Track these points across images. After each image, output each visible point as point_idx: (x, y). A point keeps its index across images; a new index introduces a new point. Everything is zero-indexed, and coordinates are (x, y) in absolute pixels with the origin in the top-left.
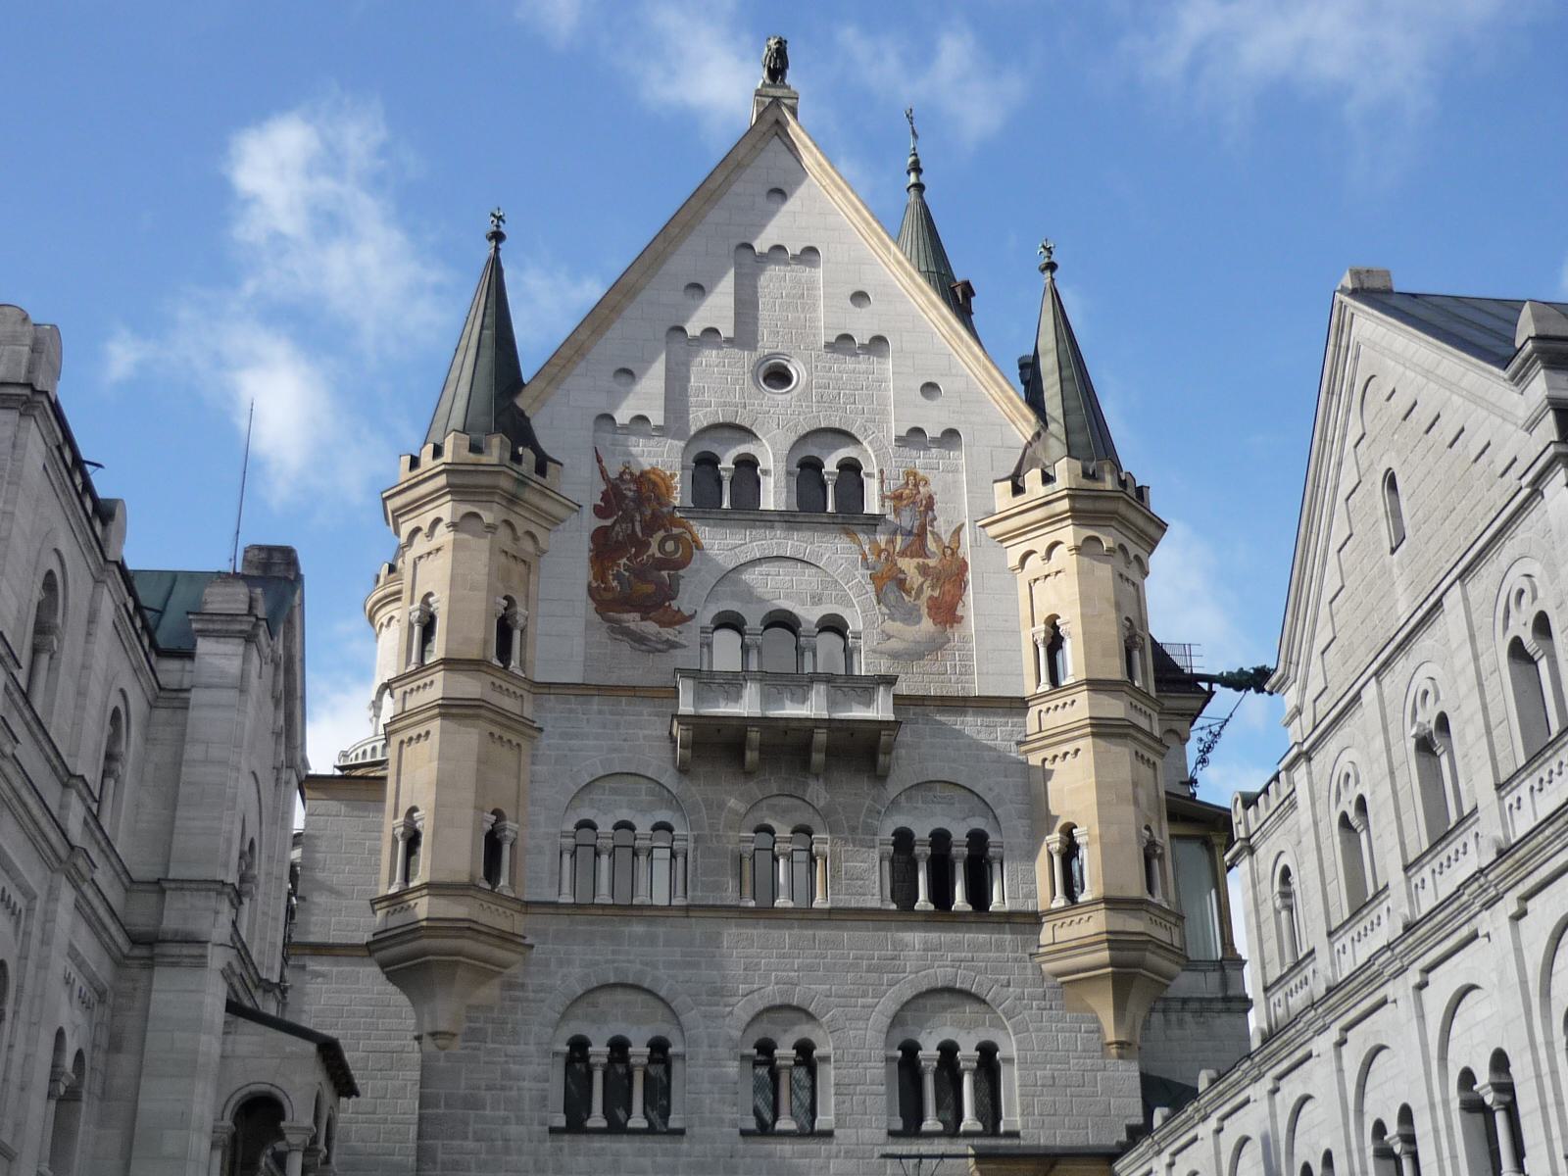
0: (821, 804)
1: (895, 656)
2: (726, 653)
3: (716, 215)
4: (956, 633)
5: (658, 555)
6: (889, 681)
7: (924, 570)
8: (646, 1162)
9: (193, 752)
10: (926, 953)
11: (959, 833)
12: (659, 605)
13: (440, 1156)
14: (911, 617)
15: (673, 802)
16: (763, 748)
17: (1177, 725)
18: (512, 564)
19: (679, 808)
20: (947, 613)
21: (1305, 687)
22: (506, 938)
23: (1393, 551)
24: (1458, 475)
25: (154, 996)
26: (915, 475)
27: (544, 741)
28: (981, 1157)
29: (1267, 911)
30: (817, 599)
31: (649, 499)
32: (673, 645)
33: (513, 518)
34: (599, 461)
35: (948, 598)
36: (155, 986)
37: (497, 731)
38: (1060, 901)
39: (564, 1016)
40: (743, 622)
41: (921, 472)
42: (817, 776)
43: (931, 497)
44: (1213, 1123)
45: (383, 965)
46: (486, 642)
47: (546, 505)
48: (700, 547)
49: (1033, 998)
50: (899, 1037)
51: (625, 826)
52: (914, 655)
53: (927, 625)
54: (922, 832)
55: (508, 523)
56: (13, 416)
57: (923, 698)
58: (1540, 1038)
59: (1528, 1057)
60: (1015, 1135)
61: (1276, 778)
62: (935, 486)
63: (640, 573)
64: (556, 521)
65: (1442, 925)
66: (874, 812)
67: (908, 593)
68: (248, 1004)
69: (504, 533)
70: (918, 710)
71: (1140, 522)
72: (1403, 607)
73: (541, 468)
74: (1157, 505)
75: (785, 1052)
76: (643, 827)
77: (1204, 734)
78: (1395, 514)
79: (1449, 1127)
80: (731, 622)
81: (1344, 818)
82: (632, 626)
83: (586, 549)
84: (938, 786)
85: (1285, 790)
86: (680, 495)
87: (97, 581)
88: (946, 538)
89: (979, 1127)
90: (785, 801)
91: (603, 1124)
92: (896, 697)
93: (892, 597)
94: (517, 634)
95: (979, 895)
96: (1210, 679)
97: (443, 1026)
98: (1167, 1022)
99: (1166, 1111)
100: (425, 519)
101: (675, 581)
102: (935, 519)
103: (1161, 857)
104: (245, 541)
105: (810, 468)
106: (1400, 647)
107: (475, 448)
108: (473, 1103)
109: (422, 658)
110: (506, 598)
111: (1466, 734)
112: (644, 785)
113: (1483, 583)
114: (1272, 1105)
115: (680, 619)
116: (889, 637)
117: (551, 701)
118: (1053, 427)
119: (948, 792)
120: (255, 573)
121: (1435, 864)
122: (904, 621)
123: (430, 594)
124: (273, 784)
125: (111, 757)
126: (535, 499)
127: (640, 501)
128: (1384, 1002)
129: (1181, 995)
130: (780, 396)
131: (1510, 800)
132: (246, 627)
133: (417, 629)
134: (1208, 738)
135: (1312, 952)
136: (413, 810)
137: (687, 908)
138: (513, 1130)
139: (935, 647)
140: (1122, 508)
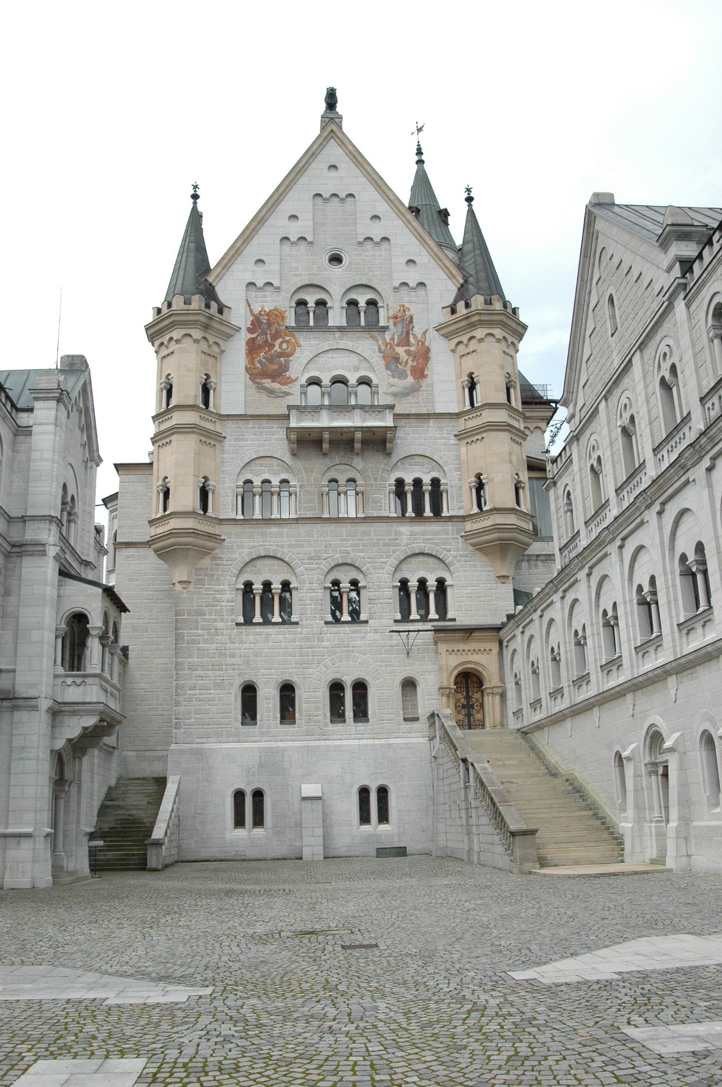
0: (359, 467)
1: (395, 395)
3: (303, 180)
4: (425, 382)
5: (279, 350)
6: (392, 407)
7: (408, 353)
8: (281, 637)
9: (36, 455)
11: (426, 480)
12: (280, 375)
13: (186, 638)
14: (402, 375)
16: (331, 442)
17: (540, 425)
18: (208, 358)
19: (292, 472)
20: (420, 373)
21: (576, 404)
23: (612, 335)
24: (639, 295)
25: (23, 570)
26: (403, 306)
27: (227, 443)
28: (437, 631)
29: (562, 511)
30: (356, 369)
31: (274, 323)
32: (287, 394)
33: (207, 336)
34: (249, 306)
35: (420, 366)
36: (23, 565)
37: (204, 439)
38: (476, 510)
39: (240, 571)
40: (321, 382)
41: (407, 305)
42: (358, 454)
43: (411, 317)
44: (539, 613)
45: (156, 551)
46: (196, 396)
47: (223, 328)
49: (462, 556)
50: (399, 576)
51: (266, 481)
52: (404, 394)
53: (410, 379)
54: (409, 479)
55: (204, 338)
57: (408, 415)
58: (668, 570)
59: (663, 579)
60: (454, 620)
61: (564, 449)
63: (271, 360)
65: (629, 517)
66: (385, 470)
67: (401, 364)
68: (73, 573)
70: (406, 421)
71: (514, 325)
72: (616, 362)
73: (220, 311)
74: (523, 317)
75: (345, 585)
76: (275, 482)
77: (553, 428)
78: (613, 316)
79: (632, 612)
80: (315, 382)
81: (592, 466)
82: (267, 385)
83: (244, 349)
84: (416, 457)
85: (568, 455)
86: (291, 321)
88: (419, 337)
89: (437, 617)
90: (343, 467)
91: (261, 620)
92: (395, 415)
93: (393, 366)
94: (211, 392)
95: (437, 509)
96: (556, 402)
97: (185, 578)
98: (530, 565)
99: (520, 607)
100: (165, 339)
101: (287, 362)
102: (413, 327)
103: (523, 488)
104: (62, 353)
105: (353, 303)
106: (614, 382)
107: (187, 302)
108: (200, 613)
109: (168, 404)
110: (206, 375)
111: (642, 426)
112: (275, 462)
113: (650, 351)
114: (562, 603)
115: (290, 381)
116: (392, 386)
118: (471, 279)
119: (421, 460)
120: (67, 368)
121: (628, 488)
122: (399, 378)
123: (169, 375)
124: (83, 469)
127: (269, 324)
128: (606, 555)
129: (536, 553)
130: (337, 270)
131: (659, 456)
132: (57, 395)
133: (165, 392)
134: (555, 430)
135: (578, 532)
136: (166, 478)
137: (297, 519)
138: (220, 625)
139: (414, 390)
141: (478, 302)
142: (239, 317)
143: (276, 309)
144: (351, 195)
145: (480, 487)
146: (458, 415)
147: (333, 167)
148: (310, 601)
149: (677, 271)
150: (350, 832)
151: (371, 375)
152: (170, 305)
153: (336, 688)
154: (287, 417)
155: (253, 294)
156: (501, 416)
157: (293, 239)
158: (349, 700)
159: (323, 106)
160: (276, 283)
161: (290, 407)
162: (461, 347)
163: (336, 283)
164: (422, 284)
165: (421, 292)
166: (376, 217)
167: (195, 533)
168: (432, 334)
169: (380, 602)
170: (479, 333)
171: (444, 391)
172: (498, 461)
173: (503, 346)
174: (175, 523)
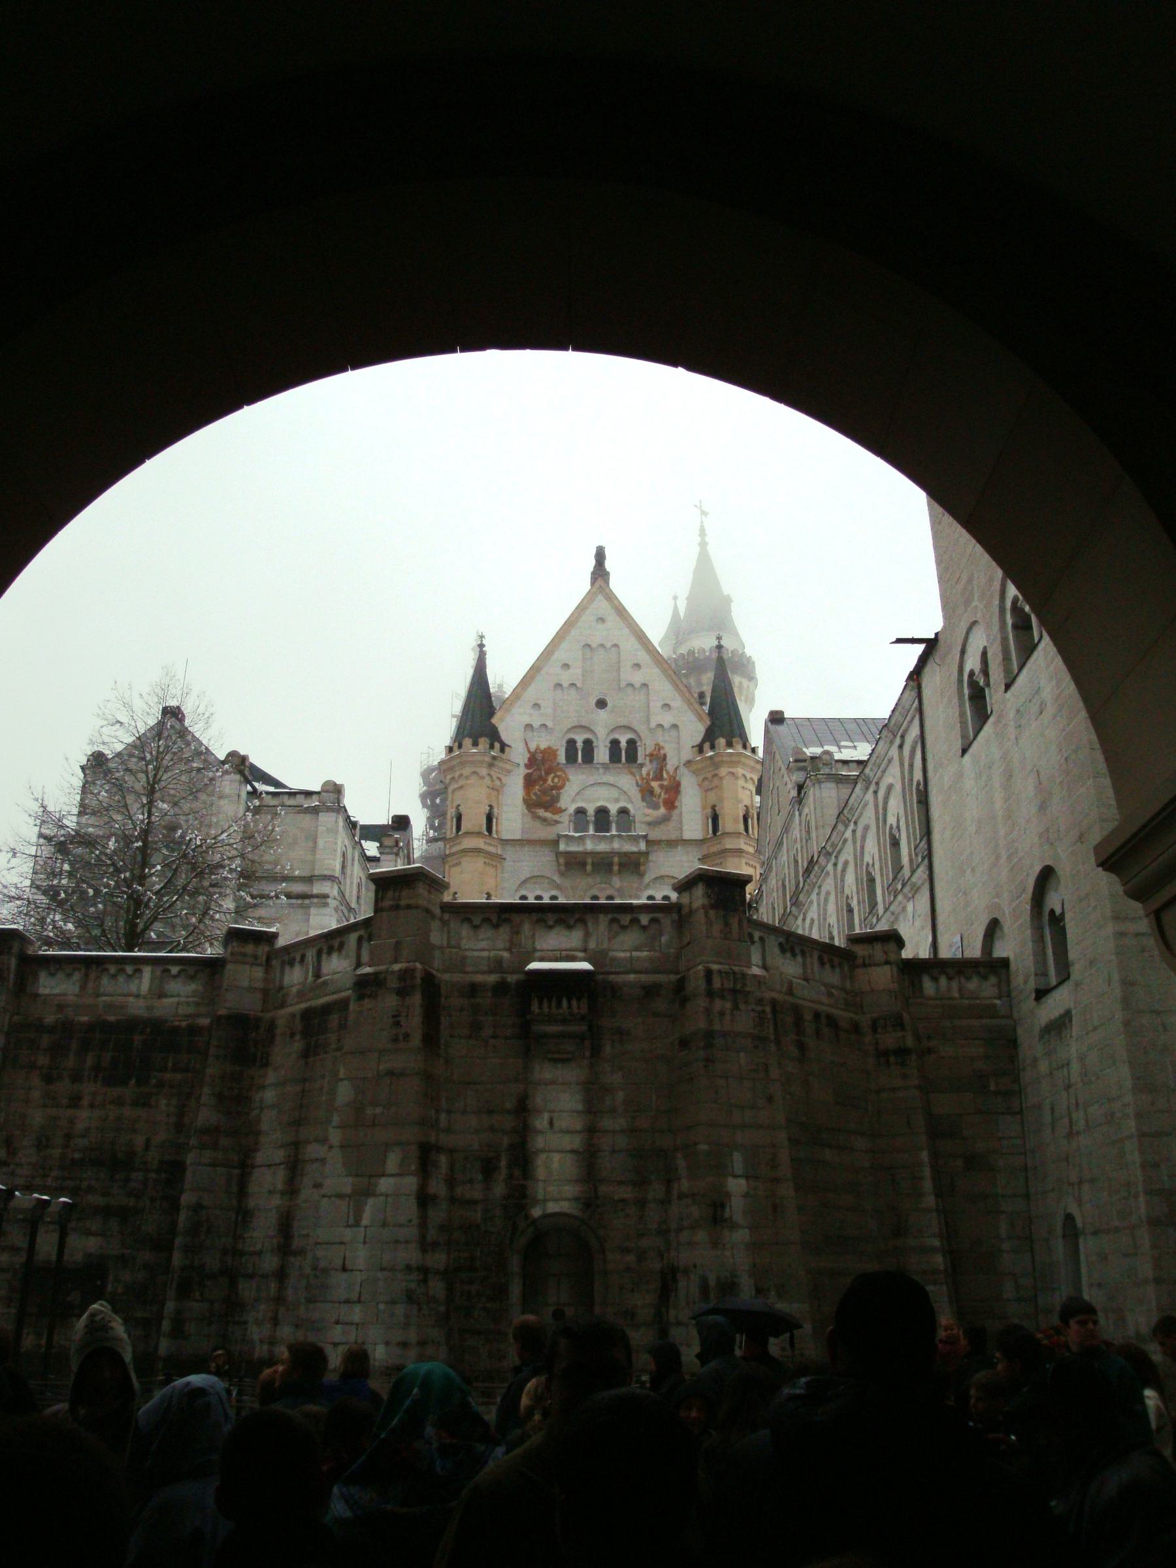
3: (574, 632)
4: (675, 812)
6: (645, 837)
7: (661, 786)
14: (656, 807)
15: (558, 887)
16: (593, 864)
20: (671, 805)
27: (506, 863)
30: (617, 800)
32: (557, 822)
33: (492, 773)
41: (662, 744)
43: (665, 755)
48: (568, 780)
56: (334, 814)
62: (669, 750)
63: (544, 792)
64: (509, 772)
66: (638, 889)
69: (487, 778)
86: (562, 757)
87: (354, 848)
92: (647, 841)
101: (558, 796)
105: (615, 743)
107: (475, 744)
117: (509, 848)
125: (358, 898)
126: (501, 764)
127: (543, 761)
130: (602, 714)
139: (666, 819)
140: (743, 759)
141: (722, 741)
143: (549, 748)
144: (616, 645)
146: (701, 842)
147: (601, 620)
149: (794, 793)
151: (629, 806)
152: (460, 746)
154: (556, 843)
155: (529, 734)
157: (565, 684)
159: (592, 563)
160: (550, 724)
161: (559, 837)
162: (706, 783)
163: (602, 727)
164: (675, 726)
165: (674, 733)
166: (637, 666)
168: (683, 770)
173: (741, 782)
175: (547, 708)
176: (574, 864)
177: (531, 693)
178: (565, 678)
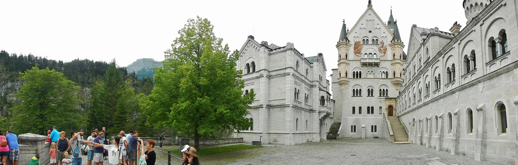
2: (366, 56)
10: (382, 82)
20: (385, 53)
22: (348, 81)
75: (370, 90)
80: (366, 54)
86: (362, 43)
105: (373, 40)
130: (370, 34)
141: (396, 40)
142: (352, 42)
145: (394, 74)
148: (365, 93)
150: (370, 134)
153: (368, 108)
156: (399, 61)
158: (370, 110)
167: (345, 81)
169: (376, 93)
170: (396, 46)
171: (389, 56)
172: (398, 69)
174: (342, 79)
175: (358, 33)
176: (364, 65)
177: (355, 31)
178: (362, 27)
